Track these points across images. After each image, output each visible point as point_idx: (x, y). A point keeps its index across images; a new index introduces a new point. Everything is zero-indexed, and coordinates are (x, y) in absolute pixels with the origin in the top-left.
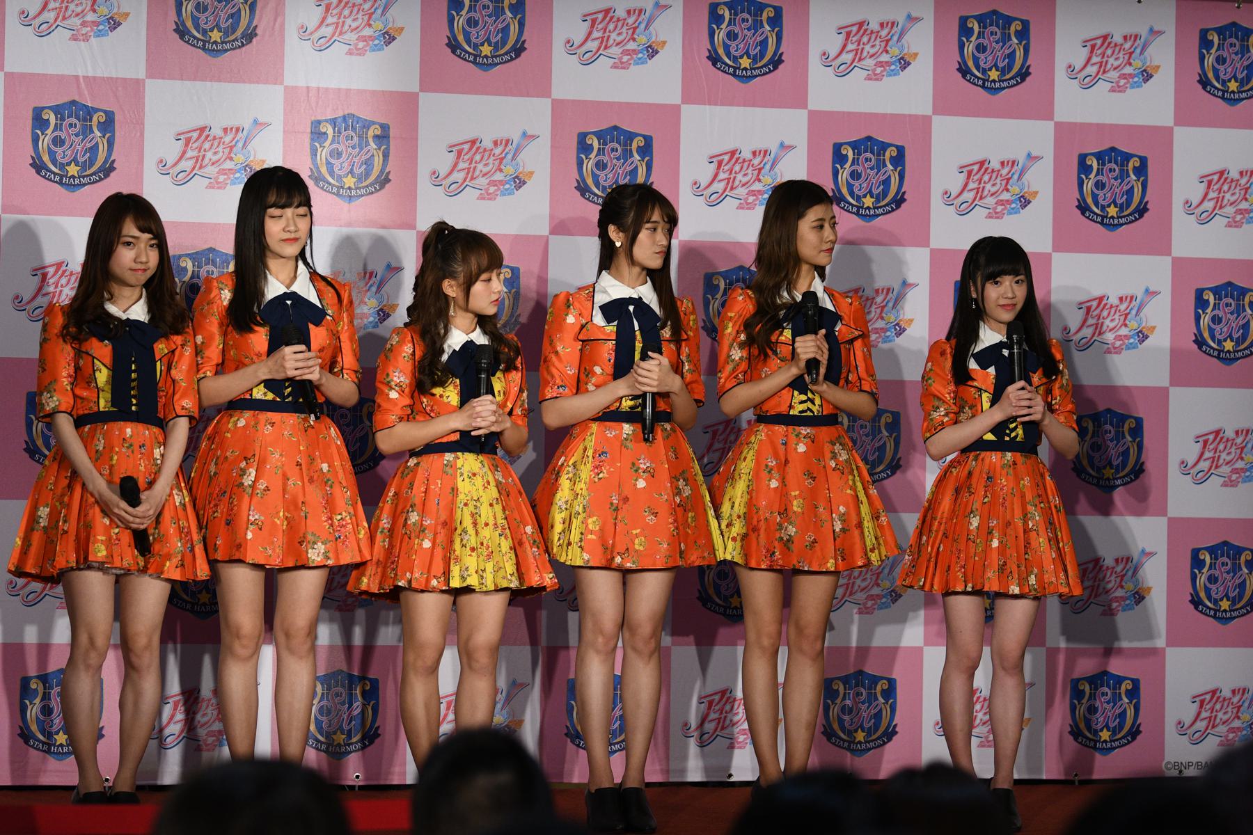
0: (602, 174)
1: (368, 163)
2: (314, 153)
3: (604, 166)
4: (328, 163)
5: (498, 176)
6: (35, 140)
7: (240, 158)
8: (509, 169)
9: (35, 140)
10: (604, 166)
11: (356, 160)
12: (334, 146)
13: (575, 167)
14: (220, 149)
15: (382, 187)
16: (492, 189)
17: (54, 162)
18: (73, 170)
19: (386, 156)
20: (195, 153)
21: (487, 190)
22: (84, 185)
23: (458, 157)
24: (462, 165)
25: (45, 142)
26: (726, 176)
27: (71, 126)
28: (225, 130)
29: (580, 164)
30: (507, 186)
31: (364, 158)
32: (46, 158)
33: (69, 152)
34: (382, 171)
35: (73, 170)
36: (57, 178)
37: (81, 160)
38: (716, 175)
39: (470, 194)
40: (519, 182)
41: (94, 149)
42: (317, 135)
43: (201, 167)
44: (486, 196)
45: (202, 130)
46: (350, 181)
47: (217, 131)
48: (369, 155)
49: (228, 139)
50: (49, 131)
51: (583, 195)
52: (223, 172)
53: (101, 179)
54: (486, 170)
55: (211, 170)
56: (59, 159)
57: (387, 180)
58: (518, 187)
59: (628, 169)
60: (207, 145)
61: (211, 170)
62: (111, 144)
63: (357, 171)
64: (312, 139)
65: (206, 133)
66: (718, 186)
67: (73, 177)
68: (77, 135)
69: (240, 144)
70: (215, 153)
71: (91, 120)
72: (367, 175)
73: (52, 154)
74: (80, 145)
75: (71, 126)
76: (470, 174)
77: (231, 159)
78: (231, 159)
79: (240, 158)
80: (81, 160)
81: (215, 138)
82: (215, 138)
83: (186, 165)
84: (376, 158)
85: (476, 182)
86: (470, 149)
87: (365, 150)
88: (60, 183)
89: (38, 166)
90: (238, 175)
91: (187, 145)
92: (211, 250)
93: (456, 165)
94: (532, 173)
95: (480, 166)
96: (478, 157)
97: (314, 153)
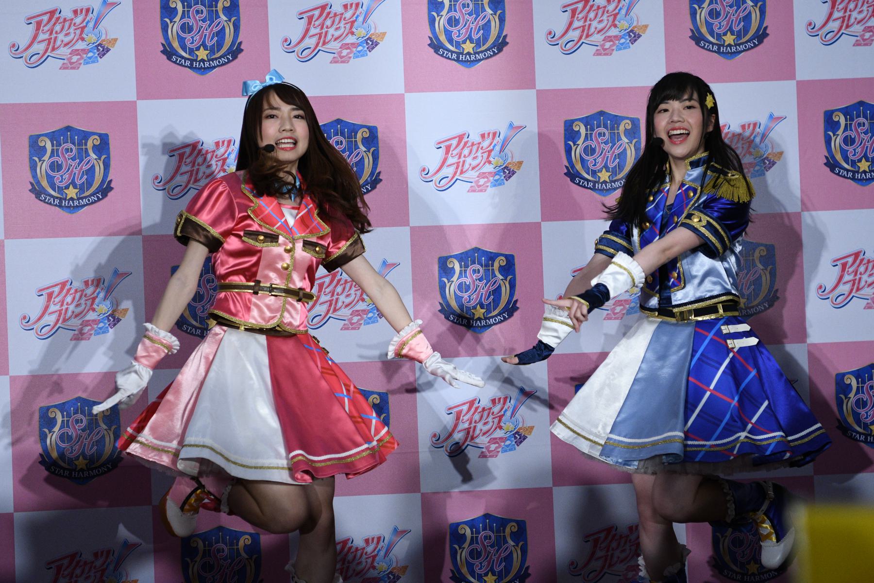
0: (716, 22)
1: (486, 27)
2: (432, 21)
3: (718, 14)
4: (446, 31)
5: (613, 32)
6: (165, 28)
7: (360, 31)
8: (623, 24)
9: (165, 28)
10: (718, 14)
11: (473, 26)
12: (450, 14)
13: (689, 17)
14: (342, 25)
15: (500, 50)
16: (608, 45)
17: (184, 48)
18: (202, 54)
19: (502, 20)
20: (318, 31)
21: (602, 46)
22: (214, 67)
23: (573, 16)
24: (576, 24)
25: (174, 29)
26: (841, 14)
27: (198, 12)
28: (345, 6)
29: (693, 14)
30: (623, 41)
31: (481, 23)
32: (176, 44)
33: (197, 38)
34: (499, 37)
35: (202, 54)
36: (188, 63)
37: (209, 44)
38: (831, 14)
39: (586, 51)
40: (634, 36)
41: (221, 33)
42: (434, 4)
43: (324, 43)
44: (603, 52)
45: (323, 8)
46: (468, 47)
47: (337, 8)
48: (486, 20)
49: (348, 15)
50: (177, 19)
51: (698, 44)
52: (346, 46)
53: (229, 61)
54: (600, 26)
55: (335, 46)
56: (188, 45)
57: (504, 43)
58: (633, 41)
59: (742, 15)
60: (328, 22)
61: (335, 46)
62: (237, 27)
63: (475, 37)
64: (430, 11)
65: (328, 10)
66: (834, 25)
67: (203, 60)
68: (204, 21)
69: (361, 19)
70: (337, 29)
71: (216, 7)
72: (485, 39)
73: (181, 41)
74: (208, 31)
75: (198, 12)
76: (586, 32)
77: (353, 33)
78: (353, 33)
79: (360, 31)
80: (209, 44)
81: (335, 15)
82: (335, 15)
83: (310, 42)
84: (493, 24)
85: (590, 39)
86: (584, 7)
87: (482, 15)
88: (191, 67)
89: (169, 53)
90: (360, 48)
91: (309, 23)
92: (339, 121)
93: (571, 24)
94: (646, 26)
95: (595, 24)
96: (592, 15)
97: (432, 21)
